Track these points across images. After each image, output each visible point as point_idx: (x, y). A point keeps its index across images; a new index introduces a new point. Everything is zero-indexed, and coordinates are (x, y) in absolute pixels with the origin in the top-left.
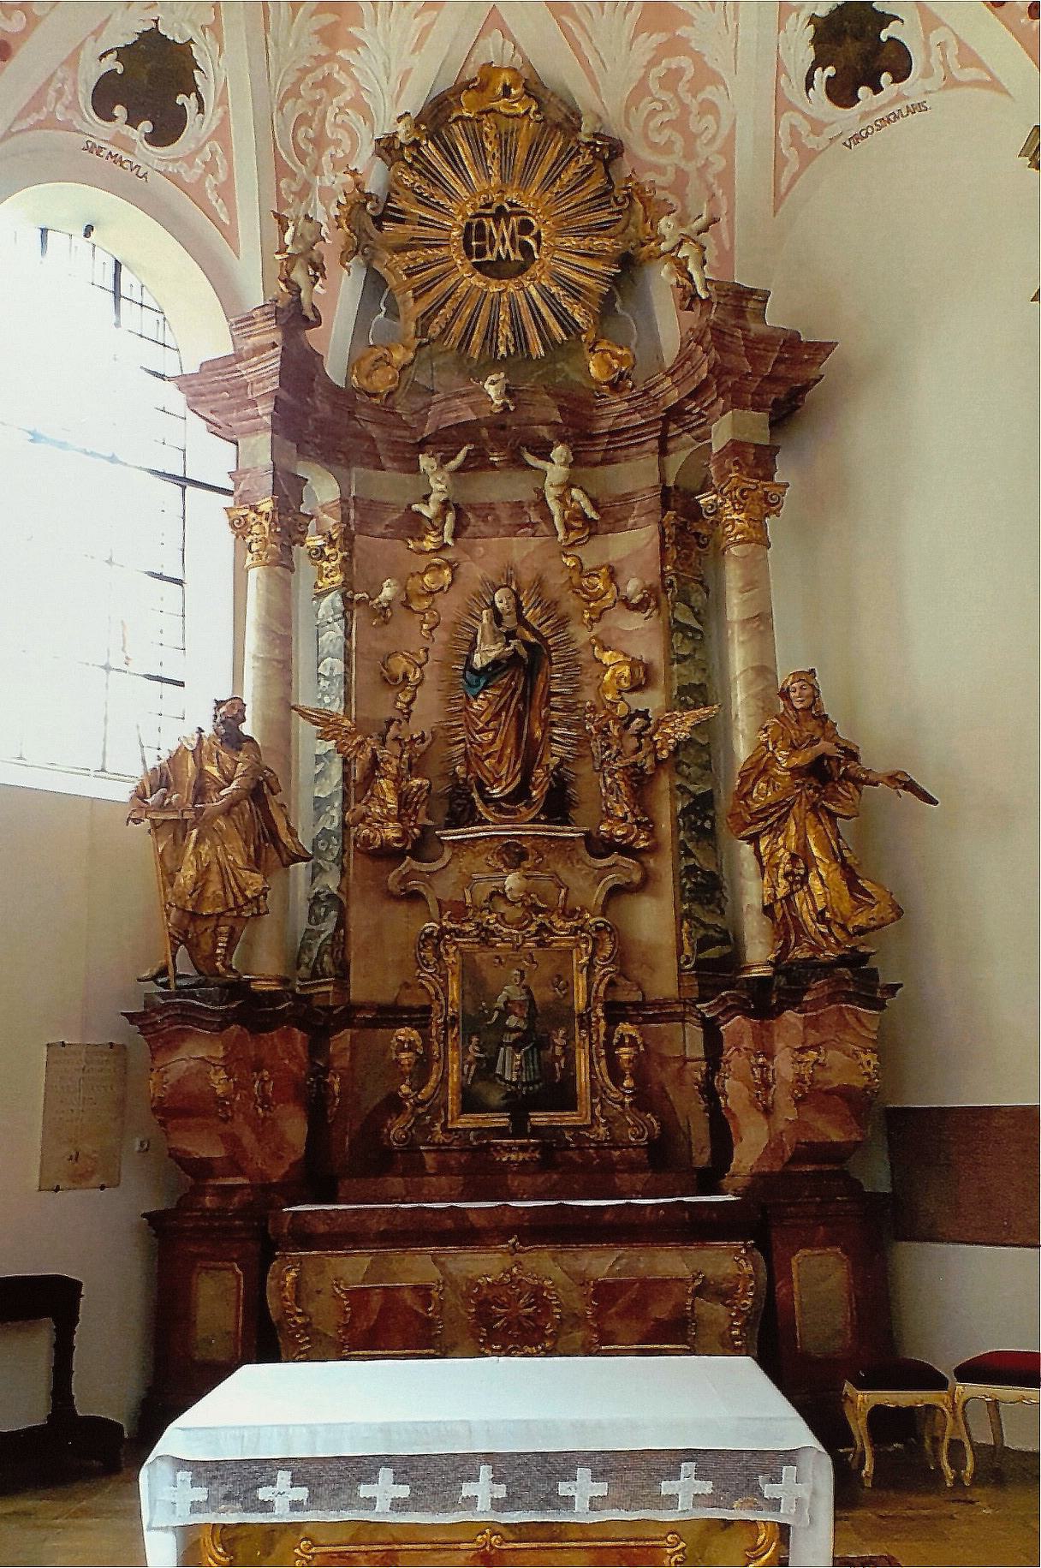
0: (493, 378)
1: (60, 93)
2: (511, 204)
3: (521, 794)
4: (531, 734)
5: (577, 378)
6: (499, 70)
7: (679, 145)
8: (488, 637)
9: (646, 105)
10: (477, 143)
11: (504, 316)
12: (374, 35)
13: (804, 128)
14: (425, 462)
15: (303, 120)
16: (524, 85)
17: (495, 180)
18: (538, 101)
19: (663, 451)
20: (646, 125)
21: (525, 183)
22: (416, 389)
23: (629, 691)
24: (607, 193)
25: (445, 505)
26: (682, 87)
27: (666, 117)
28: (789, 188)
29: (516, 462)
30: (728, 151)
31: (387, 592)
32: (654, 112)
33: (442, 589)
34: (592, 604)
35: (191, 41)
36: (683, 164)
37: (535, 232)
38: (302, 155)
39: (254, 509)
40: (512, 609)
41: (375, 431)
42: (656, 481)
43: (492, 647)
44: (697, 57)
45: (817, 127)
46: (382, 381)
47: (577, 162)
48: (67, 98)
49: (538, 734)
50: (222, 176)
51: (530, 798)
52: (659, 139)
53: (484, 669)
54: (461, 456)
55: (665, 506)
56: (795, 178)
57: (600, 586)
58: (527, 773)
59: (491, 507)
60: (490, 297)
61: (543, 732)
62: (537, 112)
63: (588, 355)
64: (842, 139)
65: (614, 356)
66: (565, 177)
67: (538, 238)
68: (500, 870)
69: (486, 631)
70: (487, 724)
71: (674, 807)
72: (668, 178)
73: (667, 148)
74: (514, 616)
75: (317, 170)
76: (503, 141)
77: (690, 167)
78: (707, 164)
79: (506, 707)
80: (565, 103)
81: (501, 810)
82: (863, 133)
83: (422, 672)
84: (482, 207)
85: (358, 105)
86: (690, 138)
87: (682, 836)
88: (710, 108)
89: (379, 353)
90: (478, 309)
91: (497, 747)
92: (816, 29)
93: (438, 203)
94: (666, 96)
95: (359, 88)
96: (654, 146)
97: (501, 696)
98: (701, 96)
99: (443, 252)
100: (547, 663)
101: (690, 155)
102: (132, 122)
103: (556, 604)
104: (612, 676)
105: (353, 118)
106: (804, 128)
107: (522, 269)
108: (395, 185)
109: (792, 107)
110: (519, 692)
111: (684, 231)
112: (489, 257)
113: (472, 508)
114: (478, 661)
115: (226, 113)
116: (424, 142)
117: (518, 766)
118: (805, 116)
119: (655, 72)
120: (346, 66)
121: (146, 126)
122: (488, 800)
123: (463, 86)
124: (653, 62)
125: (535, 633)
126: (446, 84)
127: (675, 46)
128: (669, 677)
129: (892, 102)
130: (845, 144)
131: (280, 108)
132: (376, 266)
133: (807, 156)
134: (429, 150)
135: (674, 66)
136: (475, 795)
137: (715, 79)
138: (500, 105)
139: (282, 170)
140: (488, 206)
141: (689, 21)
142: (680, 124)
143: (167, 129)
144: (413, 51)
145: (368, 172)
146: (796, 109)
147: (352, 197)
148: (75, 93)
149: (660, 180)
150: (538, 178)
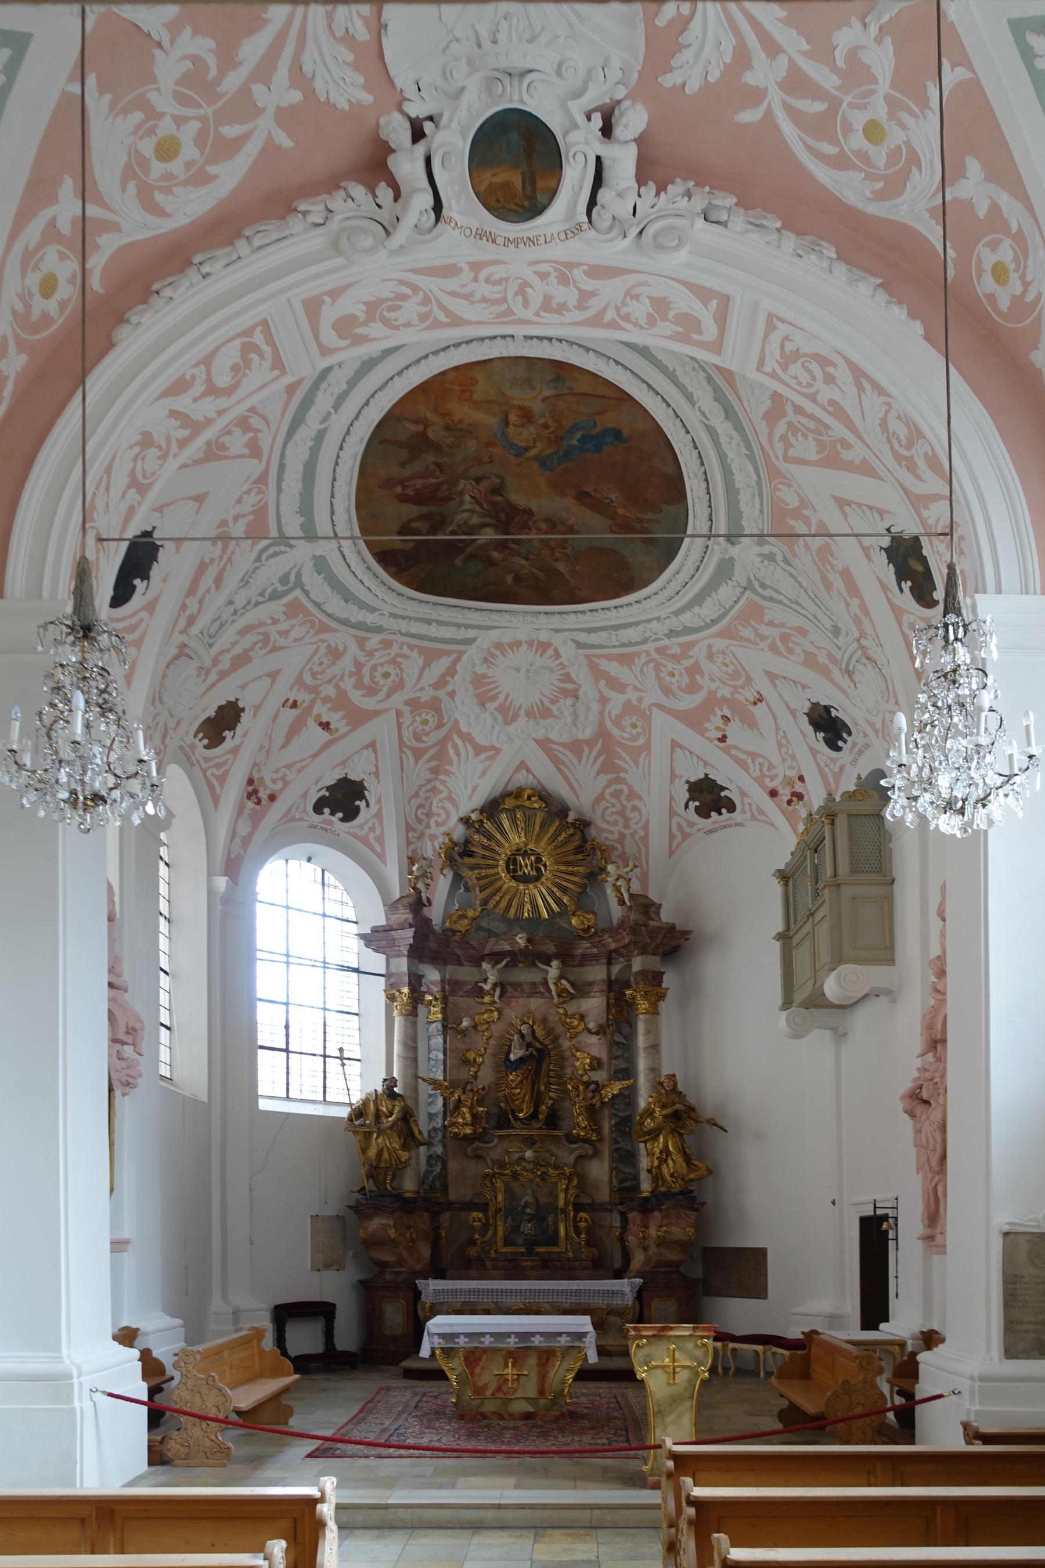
0: (520, 936)
13: (684, 824)
15: (421, 806)
21: (539, 838)
22: (480, 928)
24: (582, 847)
25: (495, 985)
28: (677, 848)
38: (419, 821)
45: (691, 824)
52: (611, 819)
54: (504, 963)
56: (679, 845)
66: (560, 839)
90: (514, 896)
99: (492, 871)
106: (684, 824)
107: (537, 878)
109: (678, 815)
111: (619, 873)
112: (520, 873)
113: (511, 984)
131: (409, 802)
133: (686, 836)
134: (488, 825)
139: (409, 828)
140: (519, 850)
150: (546, 839)
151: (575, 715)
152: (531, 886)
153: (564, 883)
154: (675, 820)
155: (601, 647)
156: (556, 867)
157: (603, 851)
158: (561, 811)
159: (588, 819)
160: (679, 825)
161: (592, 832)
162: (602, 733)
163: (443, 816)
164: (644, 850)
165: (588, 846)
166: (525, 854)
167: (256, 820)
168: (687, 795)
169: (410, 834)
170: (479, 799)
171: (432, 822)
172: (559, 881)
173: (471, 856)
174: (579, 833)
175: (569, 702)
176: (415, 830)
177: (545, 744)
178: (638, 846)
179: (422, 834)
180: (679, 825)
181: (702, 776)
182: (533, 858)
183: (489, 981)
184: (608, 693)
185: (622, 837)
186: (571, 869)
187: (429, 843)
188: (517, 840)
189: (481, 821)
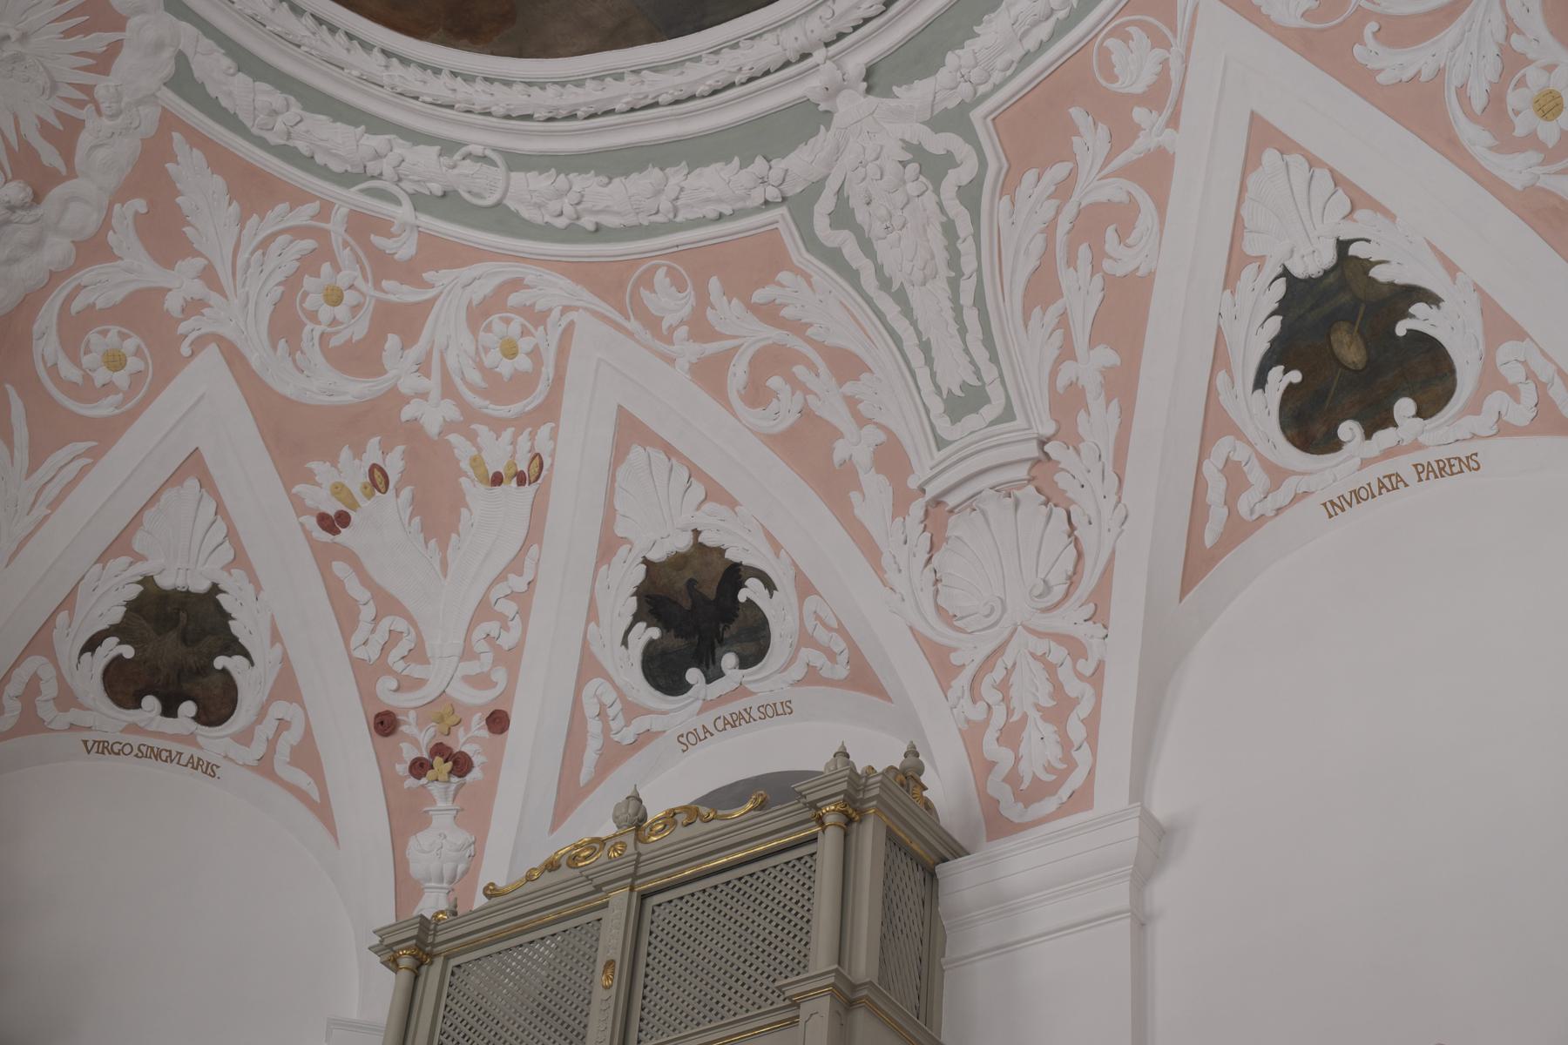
45: (67, 699)
64: (86, 735)
82: (117, 748)
118: (60, 678)
129: (176, 738)
130: (85, 742)
155: (230, 120)
168: (116, 615)
180: (35, 680)
181: (201, 586)
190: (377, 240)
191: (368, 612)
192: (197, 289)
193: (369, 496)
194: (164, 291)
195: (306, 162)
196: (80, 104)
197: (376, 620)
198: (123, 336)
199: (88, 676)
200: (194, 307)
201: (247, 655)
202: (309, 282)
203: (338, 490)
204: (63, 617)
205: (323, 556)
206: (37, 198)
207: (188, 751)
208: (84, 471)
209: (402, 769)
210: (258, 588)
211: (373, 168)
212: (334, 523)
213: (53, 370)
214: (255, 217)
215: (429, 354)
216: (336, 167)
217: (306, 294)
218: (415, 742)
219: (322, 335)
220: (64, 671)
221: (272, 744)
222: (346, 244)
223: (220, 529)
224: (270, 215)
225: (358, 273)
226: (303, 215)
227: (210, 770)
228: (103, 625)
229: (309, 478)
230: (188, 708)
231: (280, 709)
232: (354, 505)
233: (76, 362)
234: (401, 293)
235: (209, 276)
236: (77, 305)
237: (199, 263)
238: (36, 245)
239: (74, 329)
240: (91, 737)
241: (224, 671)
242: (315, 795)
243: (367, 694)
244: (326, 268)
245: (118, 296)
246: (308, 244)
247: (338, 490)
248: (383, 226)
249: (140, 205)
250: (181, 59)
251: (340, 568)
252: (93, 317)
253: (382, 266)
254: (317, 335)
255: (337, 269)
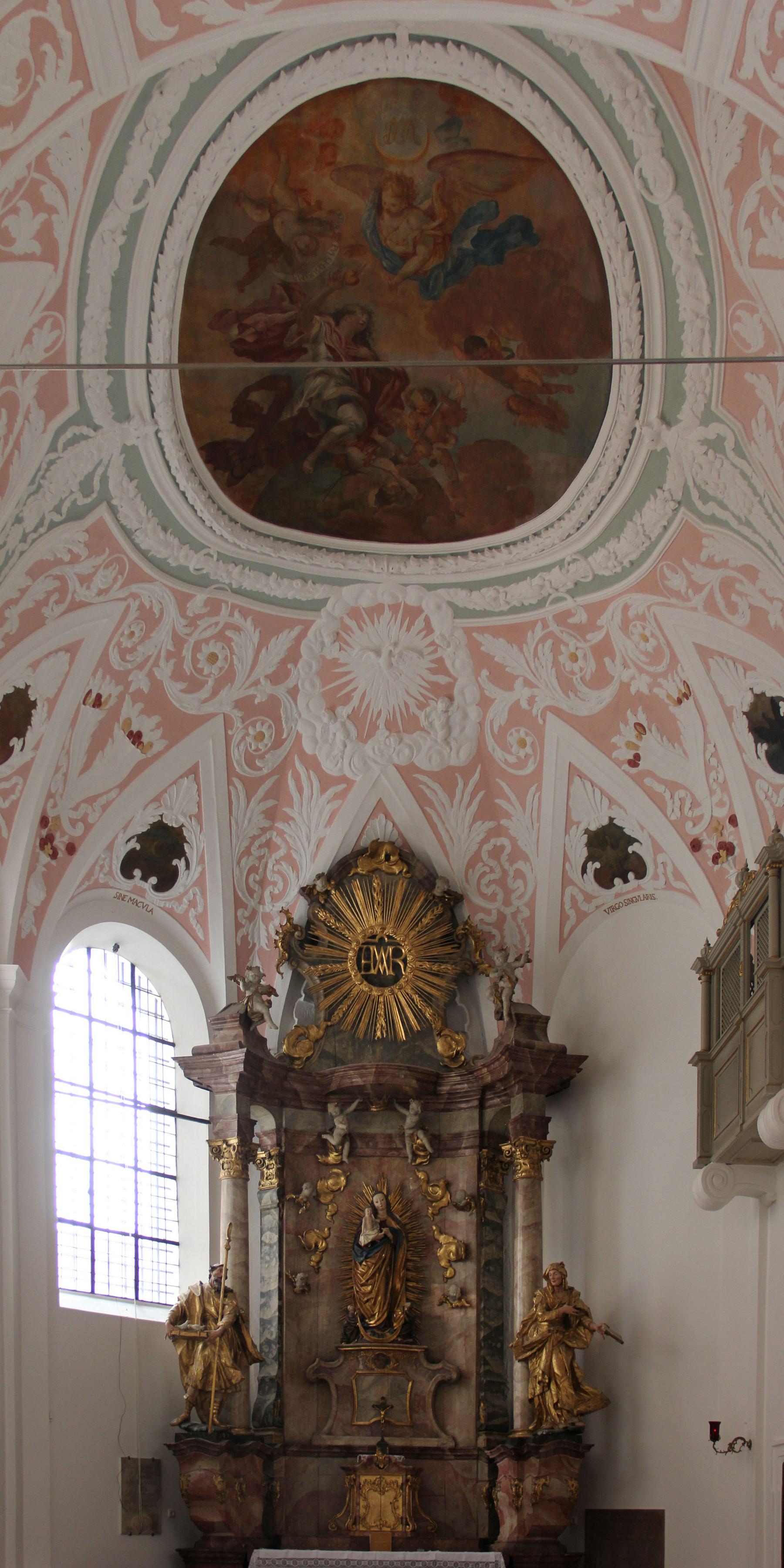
1: (102, 867)
2: (389, 937)
3: (388, 1323)
4: (394, 1286)
5: (429, 1051)
6: (383, 844)
7: (500, 897)
8: (369, 1226)
9: (480, 868)
10: (368, 890)
11: (381, 1012)
12: (301, 814)
13: (580, 898)
14: (332, 1109)
15: (253, 870)
16: (400, 855)
17: (380, 920)
18: (408, 864)
19: (482, 1107)
20: (479, 879)
23: (456, 1261)
24: (451, 934)
26: (504, 857)
27: (492, 877)
29: (389, 1107)
30: (531, 905)
31: (306, 1192)
32: (484, 874)
33: (340, 1189)
34: (434, 1204)
35: (183, 826)
36: (502, 909)
37: (403, 957)
38: (251, 892)
39: (226, 1142)
40: (384, 1206)
41: (297, 1086)
42: (476, 1127)
43: (371, 1232)
44: (514, 841)
45: (588, 898)
46: (301, 1051)
47: (433, 911)
48: (106, 869)
49: (398, 1286)
50: (200, 909)
51: (393, 1327)
53: (366, 1246)
55: (481, 1147)
57: (440, 1192)
58: (391, 1312)
59: (373, 1137)
60: (372, 998)
61: (402, 1286)
62: (407, 872)
63: (436, 1038)
65: (452, 1039)
66: (425, 921)
67: (405, 961)
68: (372, 1369)
69: (368, 1222)
70: (367, 1281)
71: (478, 1335)
72: (493, 918)
73: (493, 898)
74: (385, 1211)
75: (261, 901)
76: (386, 892)
77: (508, 911)
78: (518, 911)
79: (379, 1269)
80: (426, 868)
81: (374, 1334)
83: (327, 1244)
84: (369, 938)
85: (288, 858)
86: (508, 892)
87: (482, 1353)
88: (519, 874)
89: (301, 1031)
91: (373, 1295)
92: (589, 838)
93: (341, 933)
94: (493, 863)
95: (289, 848)
96: (483, 896)
97: (376, 1264)
98: (515, 866)
100: (405, 1242)
101: (507, 902)
102: (145, 878)
103: (412, 1202)
104: (445, 1251)
105: (285, 867)
106: (580, 898)
108: (312, 918)
109: (572, 883)
110: (387, 1260)
112: (373, 972)
114: (363, 1240)
115: (204, 870)
116: (333, 892)
117: (385, 1308)
119: (487, 847)
120: (281, 833)
121: (153, 880)
122: (367, 1327)
123: (358, 853)
124: (485, 841)
125: (398, 1222)
126: (348, 851)
127: (498, 831)
128: (479, 1253)
129: (634, 890)
131: (239, 863)
132: (299, 970)
133: (582, 916)
135: (499, 844)
136: (359, 1324)
137: (526, 858)
138: (384, 867)
139: (238, 904)
140: (374, 937)
141: (509, 816)
142: (502, 882)
143: (166, 881)
144: (326, 826)
145: (295, 903)
146: (575, 885)
147: (285, 928)
148: (111, 867)
149: (487, 919)
151: (448, 726)
152: (387, 991)
153: (428, 989)
154: (569, 890)
155: (485, 614)
156: (418, 964)
157: (477, 939)
158: (427, 878)
159: (460, 892)
160: (573, 899)
161: (465, 912)
162: (481, 756)
163: (280, 885)
164: (528, 939)
165: (460, 931)
166: (381, 944)
167: (51, 881)
169: (240, 912)
170: (324, 862)
171: (267, 894)
172: (421, 984)
173: (315, 944)
174: (449, 913)
175: (441, 705)
176: (245, 906)
177: (408, 772)
178: (521, 933)
179: (254, 913)
180: (573, 899)
182: (390, 949)
183: (336, 1132)
184: (491, 690)
185: (502, 917)
186: (435, 968)
187: (263, 927)
188: (372, 922)
189: (327, 893)
190: (571, 621)
191: (667, 795)
192: (527, 692)
193: (641, 739)
194: (517, 702)
195: (523, 609)
196: (435, 651)
197: (672, 797)
198: (518, 731)
199: (589, 883)
200: (531, 700)
201: (637, 841)
202: (562, 659)
203: (629, 744)
204: (567, 865)
205: (638, 780)
206: (451, 698)
207: (641, 893)
208: (539, 798)
209: (710, 863)
210: (625, 810)
211: (545, 594)
212: (634, 762)
213: (506, 762)
214: (524, 646)
215: (623, 657)
216: (534, 601)
217: (564, 665)
218: (711, 847)
219: (581, 678)
220: (582, 887)
221: (665, 874)
222: (562, 632)
223: (598, 793)
224: (529, 640)
225: (575, 641)
226: (539, 632)
227: (650, 897)
228: (583, 860)
229: (615, 747)
230: (631, 876)
231: (661, 858)
232: (637, 747)
233: (510, 753)
234: (595, 637)
235: (527, 683)
236: (496, 730)
237: (520, 680)
238: (465, 716)
239: (501, 738)
240: (605, 907)
241: (634, 852)
242: (688, 890)
243: (682, 835)
244: (563, 648)
245: (505, 715)
246: (549, 643)
247: (629, 744)
248: (568, 614)
249: (485, 673)
250: (450, 604)
251: (648, 781)
252: (504, 731)
253: (581, 631)
254: (579, 679)
255: (567, 645)
